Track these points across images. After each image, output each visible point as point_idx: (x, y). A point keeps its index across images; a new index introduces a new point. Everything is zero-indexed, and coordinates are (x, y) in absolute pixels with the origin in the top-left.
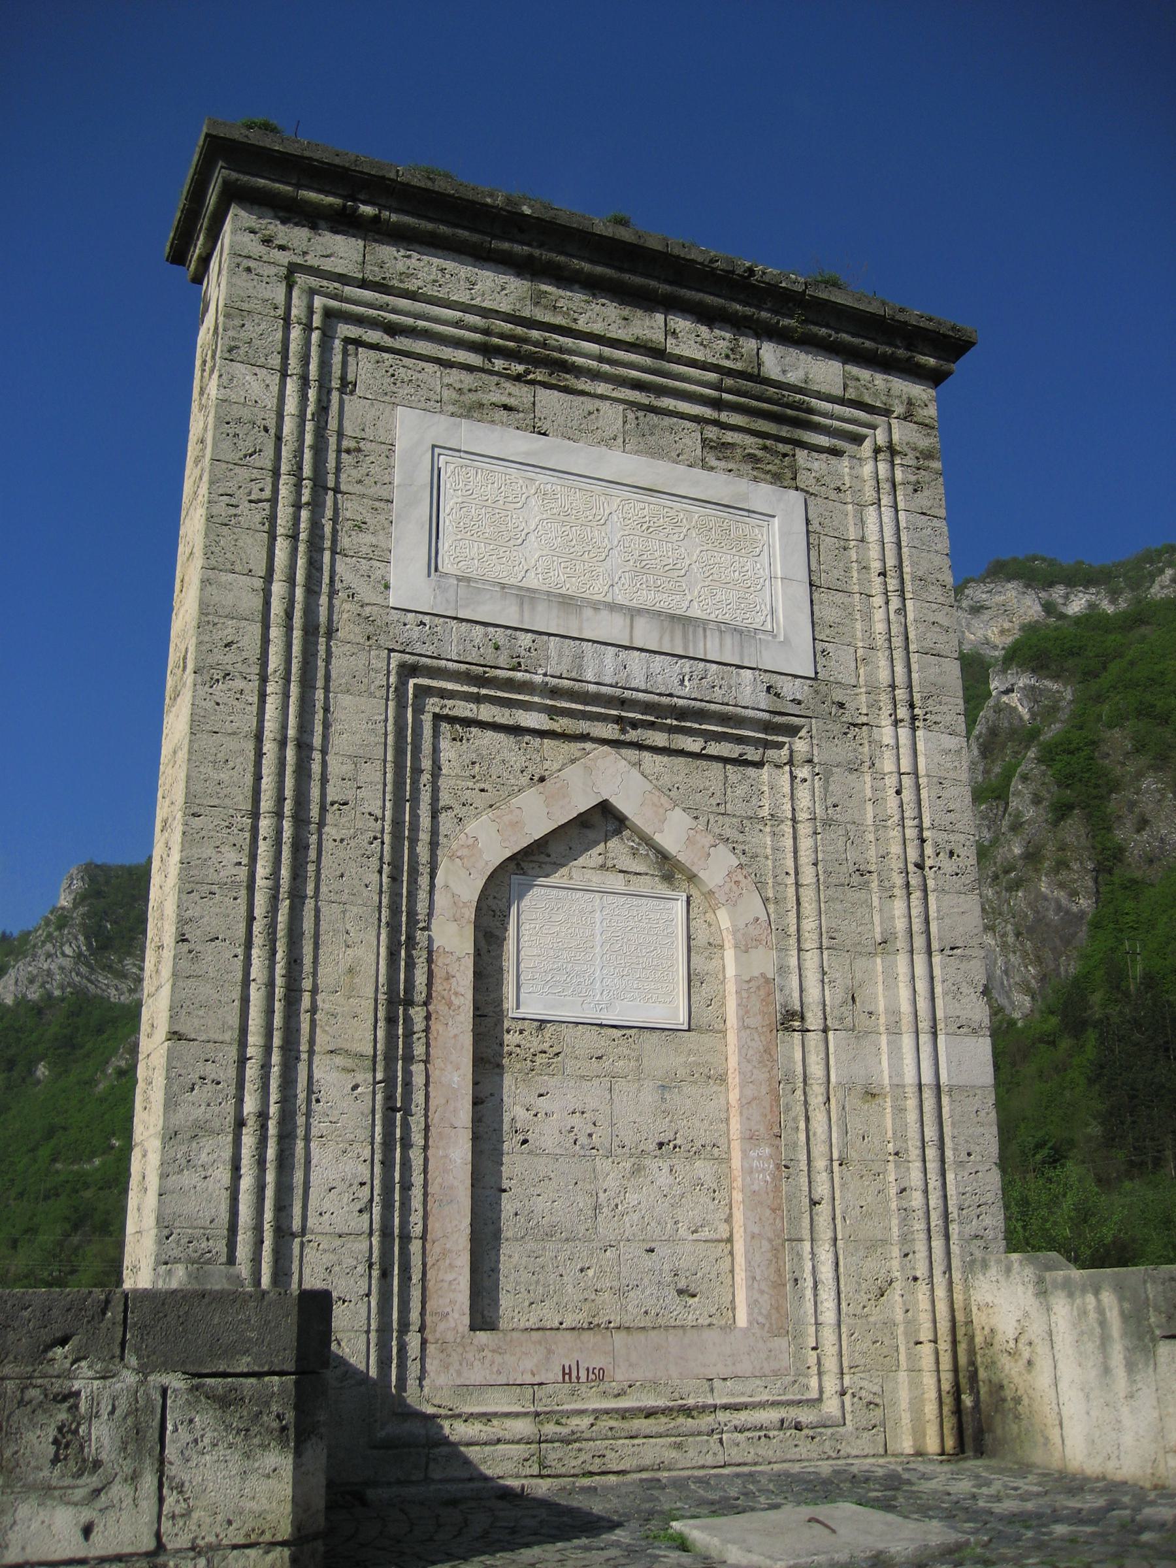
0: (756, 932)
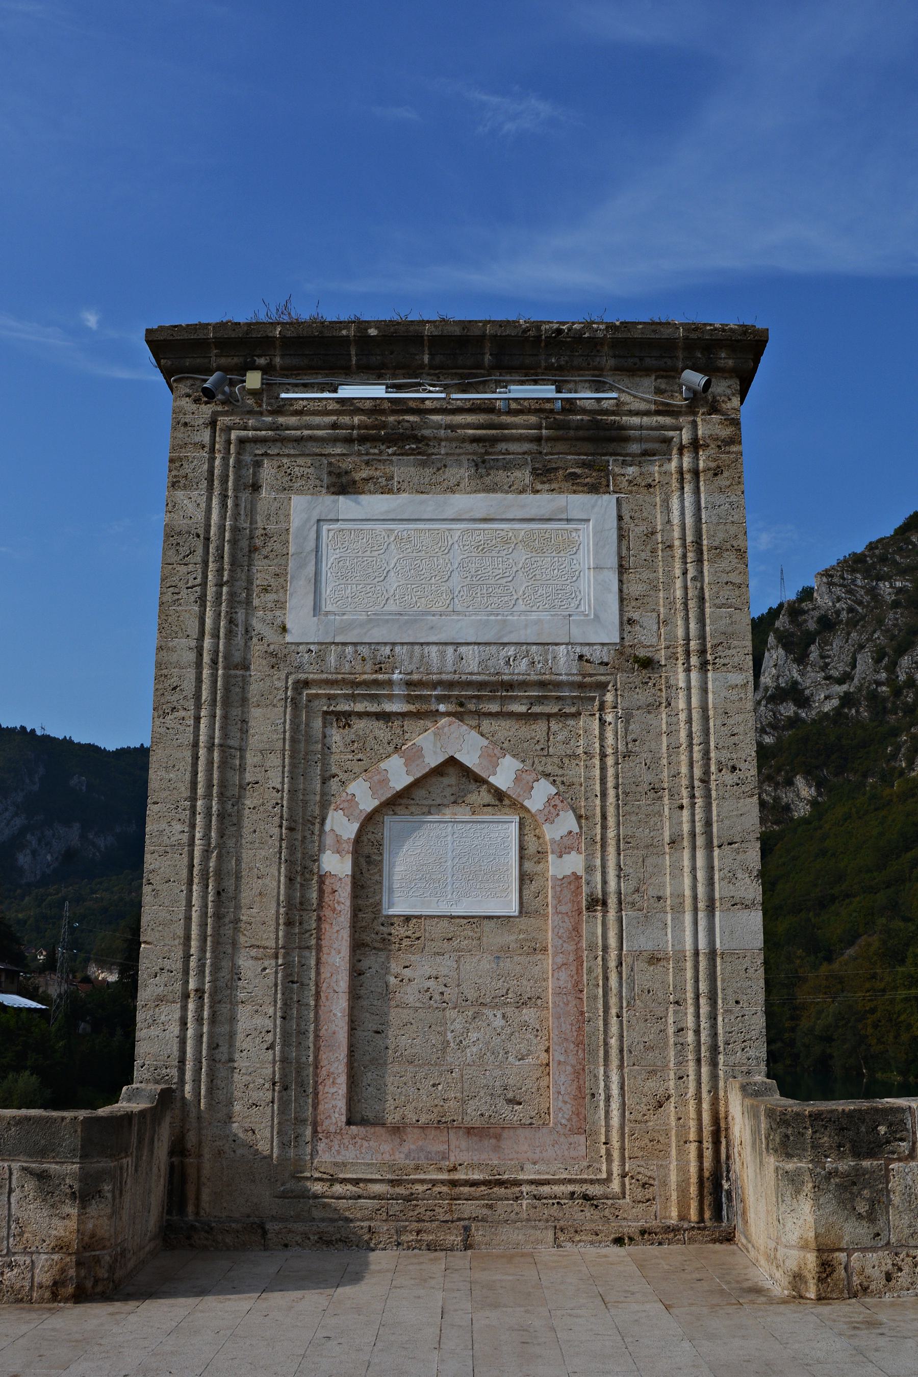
0: (569, 842)
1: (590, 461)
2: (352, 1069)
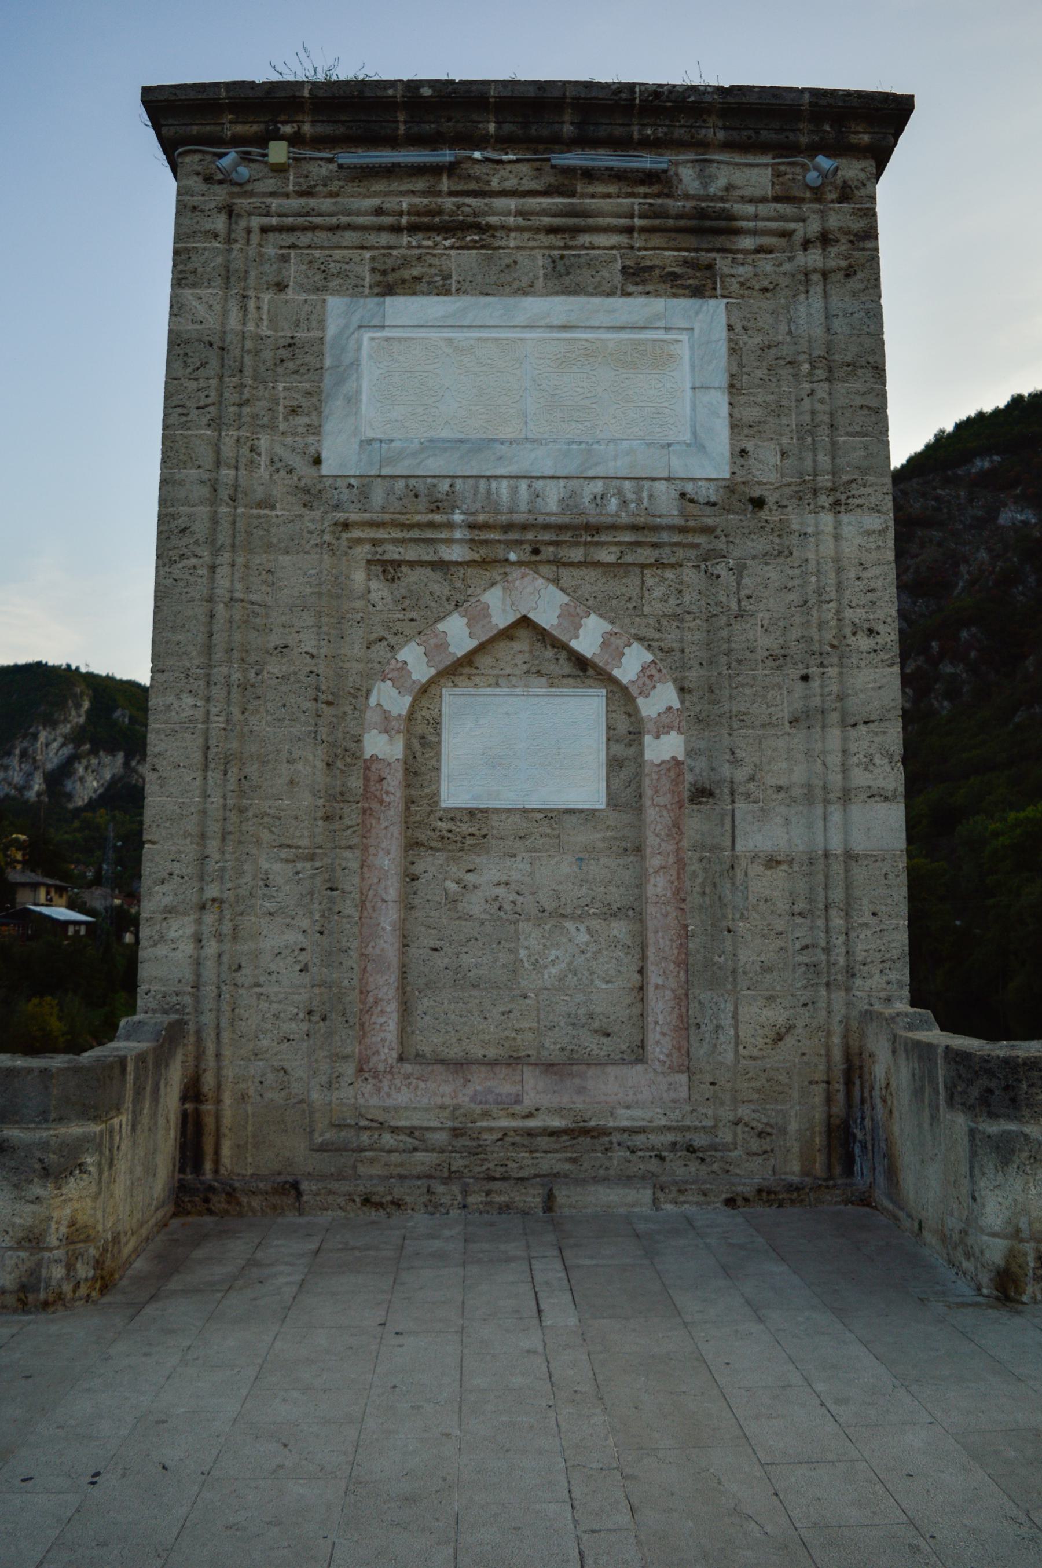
0: (668, 720)
1: (693, 258)
2: (404, 993)
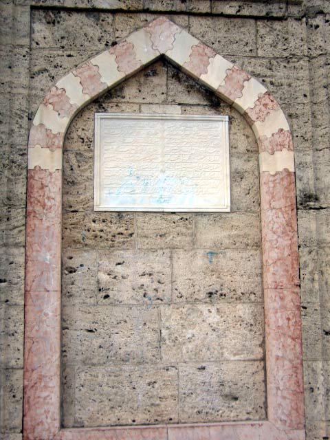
0: (280, 140)
